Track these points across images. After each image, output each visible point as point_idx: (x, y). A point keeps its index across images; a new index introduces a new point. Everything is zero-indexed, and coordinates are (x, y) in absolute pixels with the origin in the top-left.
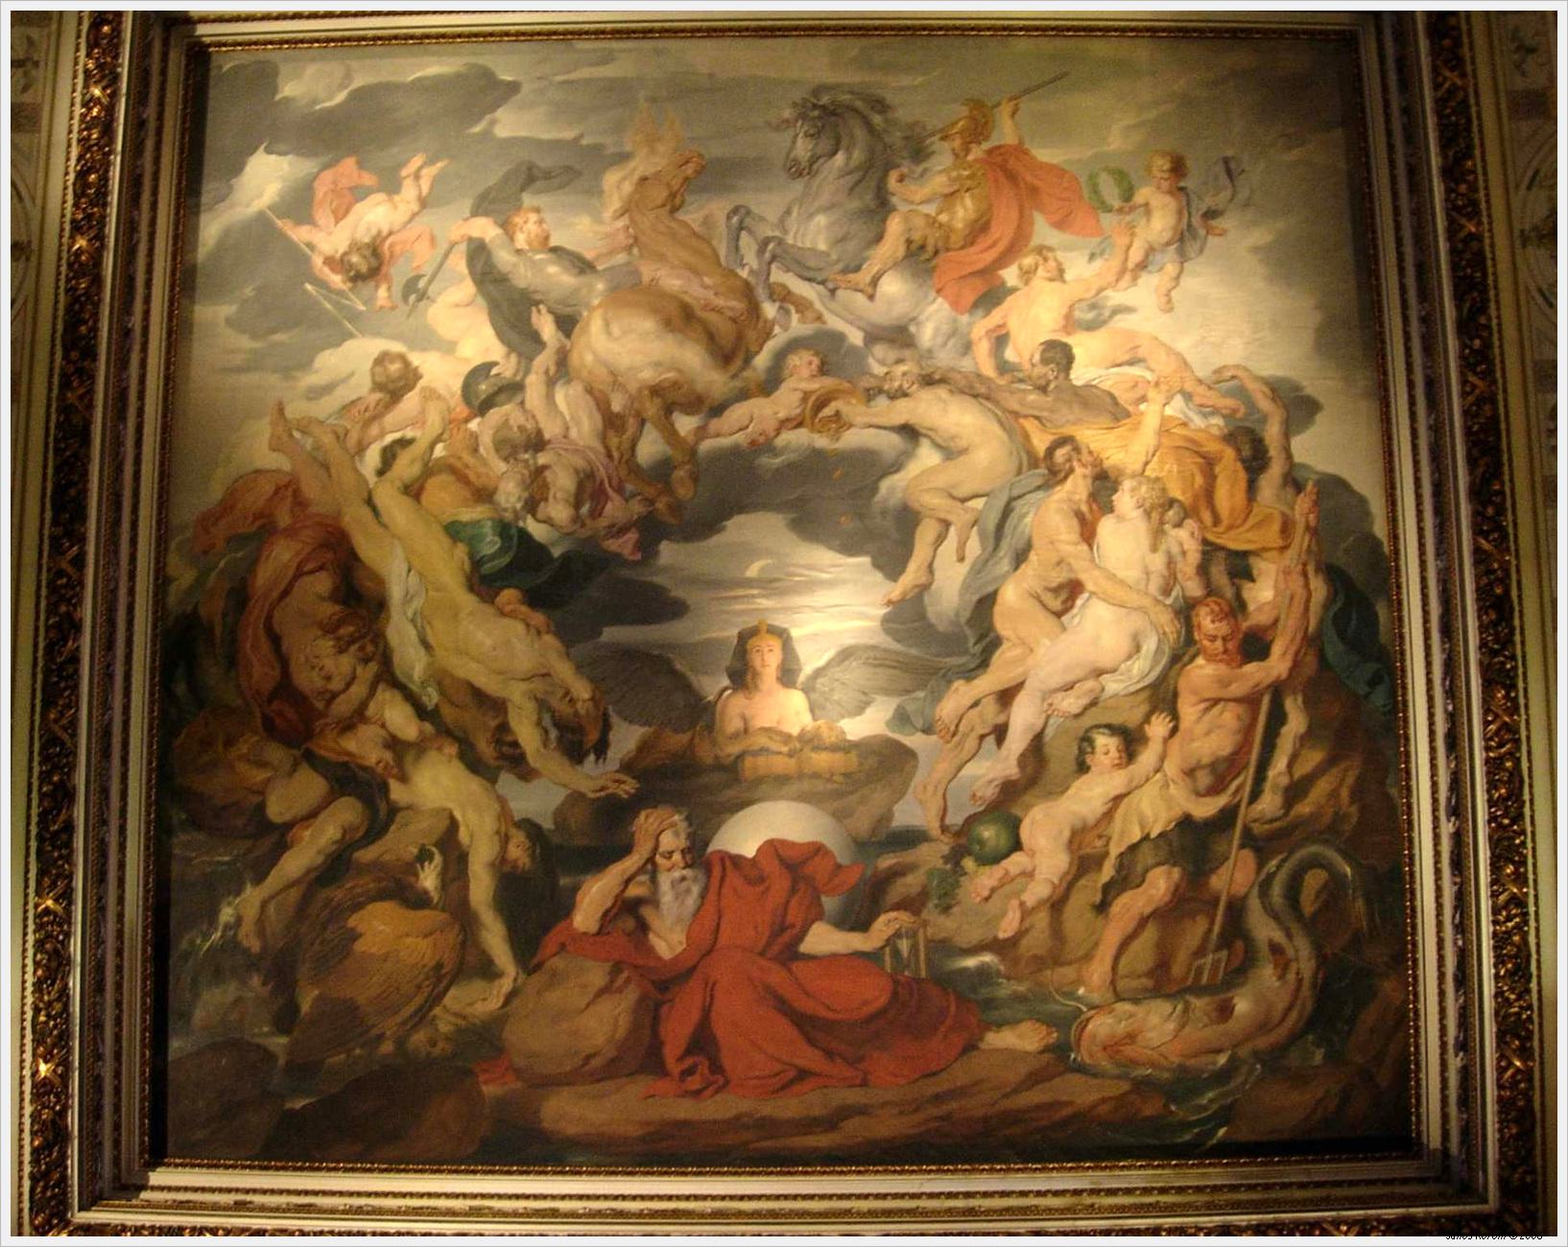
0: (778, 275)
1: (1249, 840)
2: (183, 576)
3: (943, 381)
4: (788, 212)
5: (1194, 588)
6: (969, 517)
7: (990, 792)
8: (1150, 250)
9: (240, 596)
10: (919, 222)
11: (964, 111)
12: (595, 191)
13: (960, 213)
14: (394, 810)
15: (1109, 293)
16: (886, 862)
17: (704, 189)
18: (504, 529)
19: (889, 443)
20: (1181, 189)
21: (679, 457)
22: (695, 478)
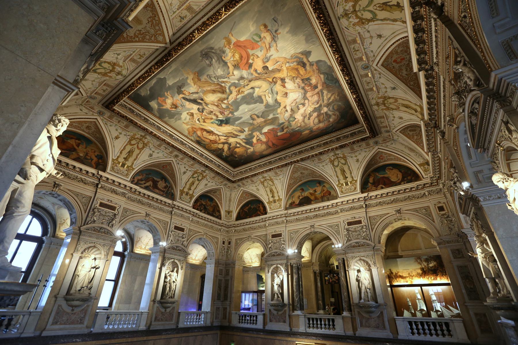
0: (220, 80)
1: (324, 106)
2: (193, 138)
3: (252, 80)
4: (214, 72)
5: (303, 85)
6: (267, 93)
7: (289, 116)
8: (269, 44)
9: (199, 137)
10: (232, 62)
11: (224, 40)
12: (189, 84)
13: (237, 57)
14: (230, 143)
15: (267, 55)
16: (282, 126)
17: (201, 76)
18: (217, 120)
19: (251, 91)
20: (269, 30)
21: (228, 105)
22: (232, 106)
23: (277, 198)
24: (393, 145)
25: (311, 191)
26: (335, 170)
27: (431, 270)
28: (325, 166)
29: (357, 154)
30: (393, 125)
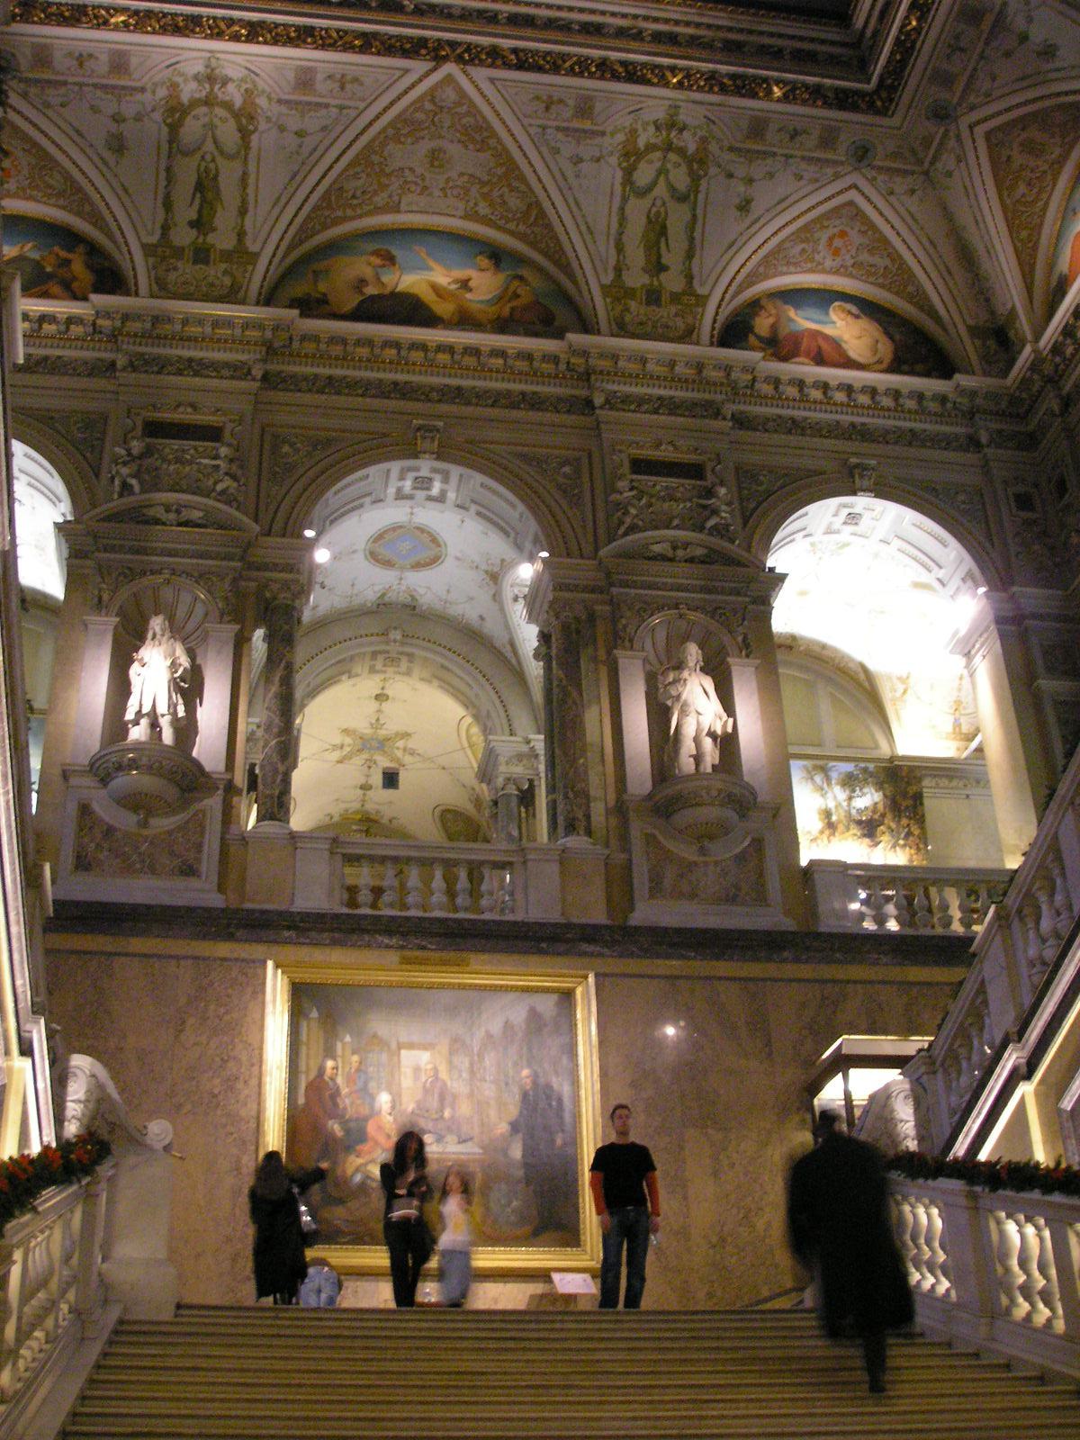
23: (222, 239)
24: (913, 204)
25: (442, 277)
26: (622, 209)
27: (859, 823)
28: (586, 167)
29: (758, 169)
30: (987, 85)
